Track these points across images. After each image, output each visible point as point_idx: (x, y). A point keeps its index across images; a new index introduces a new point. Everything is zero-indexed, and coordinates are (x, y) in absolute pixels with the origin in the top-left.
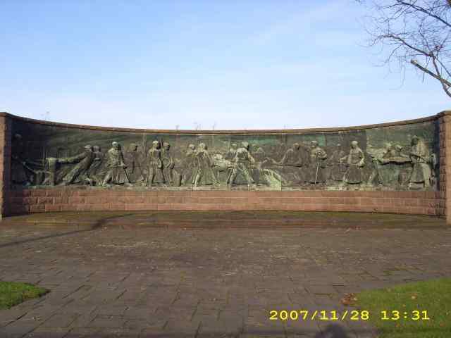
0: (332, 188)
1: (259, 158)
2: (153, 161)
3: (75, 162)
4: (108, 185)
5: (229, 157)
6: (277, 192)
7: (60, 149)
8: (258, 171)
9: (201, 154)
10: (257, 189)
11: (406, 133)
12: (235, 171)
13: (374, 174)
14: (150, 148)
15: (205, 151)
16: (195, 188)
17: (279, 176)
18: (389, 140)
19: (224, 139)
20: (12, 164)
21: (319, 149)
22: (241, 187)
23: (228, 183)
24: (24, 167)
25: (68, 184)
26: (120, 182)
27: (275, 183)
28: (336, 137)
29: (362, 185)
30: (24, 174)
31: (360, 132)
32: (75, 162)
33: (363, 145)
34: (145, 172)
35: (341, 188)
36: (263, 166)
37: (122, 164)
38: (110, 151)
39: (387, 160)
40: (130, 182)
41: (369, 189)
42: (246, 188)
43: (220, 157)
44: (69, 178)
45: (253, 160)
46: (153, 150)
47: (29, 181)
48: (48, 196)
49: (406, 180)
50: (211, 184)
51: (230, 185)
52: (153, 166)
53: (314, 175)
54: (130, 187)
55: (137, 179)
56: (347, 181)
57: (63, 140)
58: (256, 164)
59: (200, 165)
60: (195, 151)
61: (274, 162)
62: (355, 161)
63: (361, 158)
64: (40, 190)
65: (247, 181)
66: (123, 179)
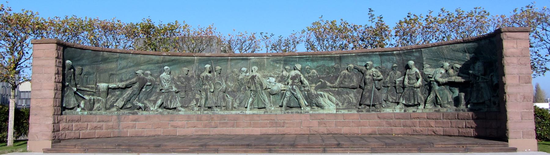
0: (389, 110)
1: (312, 80)
2: (205, 84)
3: (127, 87)
4: (160, 110)
5: (282, 79)
7: (112, 74)
8: (311, 93)
10: (311, 112)
12: (288, 94)
14: (202, 72)
16: (248, 112)
17: (334, 99)
18: (446, 59)
19: (276, 62)
22: (294, 110)
26: (172, 107)
28: (391, 57)
30: (75, 100)
31: (416, 52)
32: (127, 87)
34: (198, 96)
36: (316, 89)
37: (174, 89)
41: (427, 111)
42: (299, 111)
43: (273, 80)
44: (120, 103)
45: (306, 82)
47: (79, 106)
48: (99, 122)
52: (205, 90)
53: (370, 97)
54: (183, 111)
55: (190, 103)
57: (113, 66)
58: (311, 87)
60: (248, 74)
61: (328, 84)
63: (418, 79)
64: (92, 116)
66: (177, 104)
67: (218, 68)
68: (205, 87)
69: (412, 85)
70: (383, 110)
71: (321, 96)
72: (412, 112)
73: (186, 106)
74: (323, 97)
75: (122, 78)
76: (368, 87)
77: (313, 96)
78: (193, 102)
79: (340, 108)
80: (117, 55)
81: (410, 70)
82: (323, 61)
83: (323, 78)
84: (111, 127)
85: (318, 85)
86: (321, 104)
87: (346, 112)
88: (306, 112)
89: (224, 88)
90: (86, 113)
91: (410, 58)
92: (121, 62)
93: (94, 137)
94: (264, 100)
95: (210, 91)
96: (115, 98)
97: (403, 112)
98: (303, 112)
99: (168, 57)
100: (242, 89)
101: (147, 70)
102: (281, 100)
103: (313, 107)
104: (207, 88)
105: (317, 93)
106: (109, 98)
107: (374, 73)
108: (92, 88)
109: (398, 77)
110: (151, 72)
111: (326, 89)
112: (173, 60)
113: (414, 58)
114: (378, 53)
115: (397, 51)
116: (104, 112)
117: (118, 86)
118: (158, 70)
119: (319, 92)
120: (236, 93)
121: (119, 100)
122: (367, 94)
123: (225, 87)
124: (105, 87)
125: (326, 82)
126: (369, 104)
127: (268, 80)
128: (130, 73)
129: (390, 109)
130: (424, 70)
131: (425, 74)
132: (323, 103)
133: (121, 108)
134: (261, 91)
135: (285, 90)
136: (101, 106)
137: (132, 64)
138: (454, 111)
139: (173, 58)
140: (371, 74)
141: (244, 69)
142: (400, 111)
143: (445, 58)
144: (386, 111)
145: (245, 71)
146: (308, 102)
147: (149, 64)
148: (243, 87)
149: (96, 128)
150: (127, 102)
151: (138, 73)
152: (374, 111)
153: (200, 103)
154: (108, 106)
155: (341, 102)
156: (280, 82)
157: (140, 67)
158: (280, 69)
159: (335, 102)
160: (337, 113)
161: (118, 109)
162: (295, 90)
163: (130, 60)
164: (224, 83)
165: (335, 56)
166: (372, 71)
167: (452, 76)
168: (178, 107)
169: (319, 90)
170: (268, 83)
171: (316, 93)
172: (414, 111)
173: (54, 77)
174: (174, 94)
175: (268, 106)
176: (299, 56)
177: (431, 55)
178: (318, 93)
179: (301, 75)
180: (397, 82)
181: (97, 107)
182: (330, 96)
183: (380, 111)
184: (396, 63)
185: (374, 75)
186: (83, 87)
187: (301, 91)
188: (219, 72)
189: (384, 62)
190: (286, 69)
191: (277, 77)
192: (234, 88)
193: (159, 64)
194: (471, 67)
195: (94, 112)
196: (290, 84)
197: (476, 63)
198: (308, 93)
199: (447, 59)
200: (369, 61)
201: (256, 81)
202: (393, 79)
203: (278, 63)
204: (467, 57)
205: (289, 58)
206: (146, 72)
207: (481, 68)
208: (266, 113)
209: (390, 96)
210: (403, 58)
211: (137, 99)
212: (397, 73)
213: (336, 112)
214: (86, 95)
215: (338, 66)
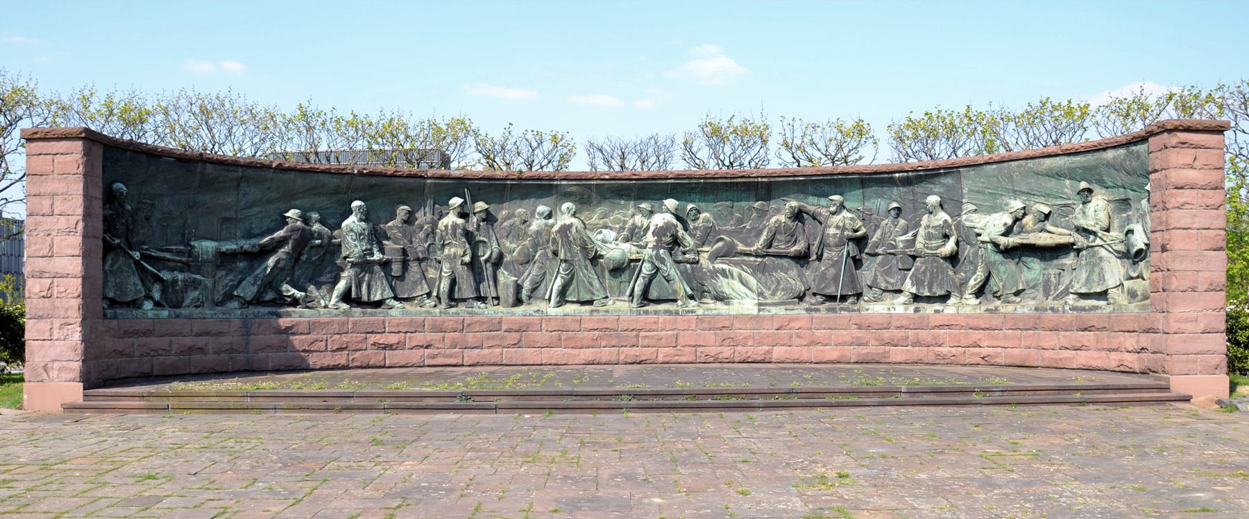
0: (879, 308)
4: (345, 306)
5: (633, 235)
6: (751, 318)
7: (226, 220)
8: (701, 268)
9: (565, 229)
10: (700, 312)
11: (1058, 175)
12: (646, 269)
13: (980, 275)
14: (441, 216)
15: (574, 220)
17: (753, 281)
18: (1016, 193)
20: (104, 260)
23: (632, 294)
24: (137, 263)
25: (246, 304)
27: (744, 302)
29: (952, 300)
30: (138, 282)
33: (951, 204)
34: (432, 273)
35: (899, 306)
36: (714, 257)
38: (346, 223)
39: (1012, 240)
40: (396, 298)
41: (968, 310)
44: (248, 290)
45: (689, 241)
46: (451, 219)
47: (149, 297)
48: (198, 335)
49: (1062, 288)
50: (590, 302)
51: (635, 304)
53: (836, 278)
55: (414, 289)
56: (914, 290)
57: (230, 199)
58: (698, 253)
59: (562, 256)
60: (551, 221)
62: (934, 243)
63: (946, 237)
64: (180, 321)
65: (675, 292)
67: (480, 205)
68: (450, 250)
70: (867, 307)
71: (724, 273)
73: (406, 296)
74: (727, 277)
75: (252, 228)
76: (833, 254)
77: (705, 273)
78: (422, 288)
79: (768, 301)
80: (237, 172)
81: (932, 216)
82: (728, 194)
83: (729, 233)
84: (228, 347)
85: (717, 249)
86: (722, 292)
87: (780, 311)
88: (689, 312)
89: (494, 256)
90: (165, 313)
91: (932, 188)
92: (247, 189)
93: (188, 371)
94: (591, 284)
95: (462, 261)
96: (234, 276)
98: (681, 310)
99: (362, 178)
100: (536, 257)
101: (312, 209)
102: (630, 283)
103: (704, 300)
104: (455, 253)
105: (714, 267)
106: (220, 278)
107: (847, 221)
108: (179, 253)
109: (900, 233)
110: (320, 214)
111: (735, 259)
112: (375, 185)
113: (941, 190)
116: (208, 312)
117: (242, 247)
118: (336, 209)
119: (719, 266)
120: (524, 267)
121: (244, 282)
122: (832, 271)
123: (496, 251)
124: (210, 250)
125: (736, 242)
127: (600, 237)
128: (270, 217)
129: (883, 306)
130: (964, 217)
132: (727, 290)
133: (250, 303)
134: (583, 262)
135: (640, 260)
136: (201, 296)
137: (274, 195)
139: (373, 180)
140: (841, 224)
141: (542, 208)
143: (1015, 191)
144: (873, 309)
145: (547, 213)
146: (692, 289)
147: (315, 195)
148: (539, 252)
149: (191, 350)
150: (265, 286)
151: (288, 217)
152: (845, 310)
153: (439, 289)
154: (218, 297)
155: (769, 289)
156: (627, 240)
157: (293, 203)
158: (628, 210)
159: (755, 288)
160: (761, 313)
161: (243, 304)
162: (663, 261)
163: (268, 186)
164: (495, 245)
165: (758, 182)
167: (1029, 232)
168: (388, 299)
169: (717, 261)
170: (600, 243)
171: (711, 267)
172: (937, 311)
173: (81, 226)
174: (377, 268)
175: (599, 295)
176: (672, 181)
177: (982, 182)
178: (716, 266)
179: (679, 224)
181: (192, 300)
182: (744, 274)
183: (859, 310)
184: (899, 199)
186: (157, 249)
187: (678, 262)
188: (483, 215)
189: (870, 198)
190: (640, 210)
191: (620, 228)
192: (519, 253)
193: (339, 196)
194: (1077, 210)
195: (184, 311)
196: (650, 245)
197: (1090, 202)
198: (692, 268)
201: (571, 239)
203: (622, 195)
204: (1067, 188)
205: (651, 184)
206: (308, 214)
207: (1103, 216)
208: (595, 314)
211: (288, 279)
213: (759, 311)
214: (164, 269)
215: (763, 205)
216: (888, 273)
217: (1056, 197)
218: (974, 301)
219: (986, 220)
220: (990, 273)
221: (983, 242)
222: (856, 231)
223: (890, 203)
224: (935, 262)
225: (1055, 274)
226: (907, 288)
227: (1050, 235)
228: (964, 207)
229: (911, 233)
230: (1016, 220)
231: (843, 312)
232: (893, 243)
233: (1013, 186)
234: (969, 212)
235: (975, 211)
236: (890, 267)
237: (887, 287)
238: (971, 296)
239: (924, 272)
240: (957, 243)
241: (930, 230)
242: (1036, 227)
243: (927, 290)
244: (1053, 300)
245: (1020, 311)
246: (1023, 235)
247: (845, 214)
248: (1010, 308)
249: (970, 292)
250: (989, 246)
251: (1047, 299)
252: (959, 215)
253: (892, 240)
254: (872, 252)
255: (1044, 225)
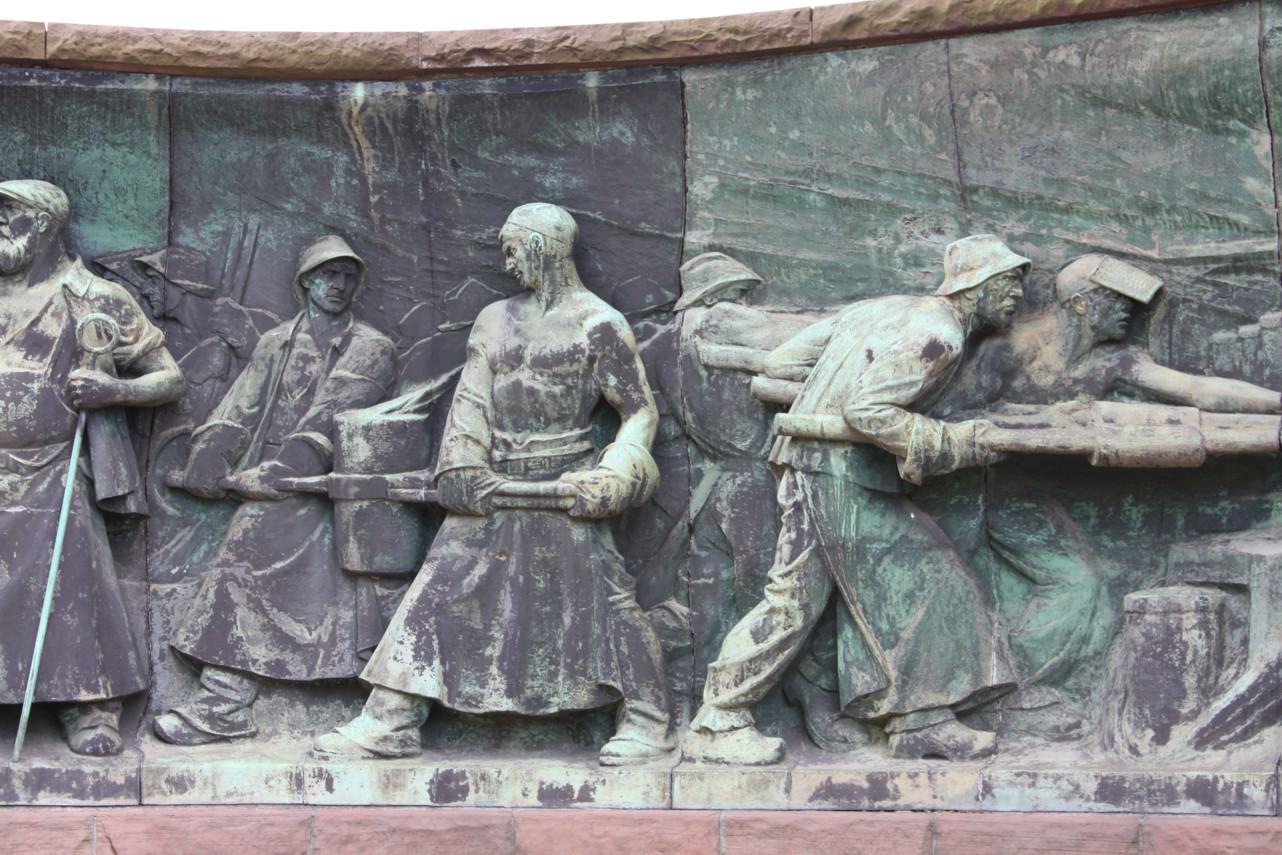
21: (75, 276)
29: (630, 740)
41: (724, 792)
56: (429, 684)
62: (545, 443)
63: (605, 418)
69: (543, 487)
72: (533, 799)
97: (425, 799)
107: (87, 316)
109: (356, 391)
114: (150, 84)
115: (391, 87)
126: (10, 698)
129: (267, 767)
130: (696, 317)
131: (690, 361)
138: (1076, 804)
140: (53, 328)
142: (389, 783)
143: (965, 194)
144: (211, 782)
166: (59, 301)
167: (1041, 397)
172: (554, 796)
177: (798, 147)
180: (360, 441)
183: (135, 787)
184: (354, 222)
185: (89, 341)
189: (207, 207)
199: (994, 193)
200: (26, 175)
202: (301, 410)
204: (1255, 170)
209: (258, 608)
210: (446, 171)
212: (355, 341)
216: (283, 592)
217: (1194, 225)
218: (753, 746)
219: (820, 327)
220: (835, 598)
221: (799, 439)
222: (129, 369)
223: (309, 241)
224: (546, 541)
225: (1202, 610)
226: (395, 669)
227: (1163, 412)
228: (692, 268)
229: (413, 395)
230: (983, 330)
231: (44, 798)
232: (321, 439)
233: (961, 166)
234: (720, 293)
235: (748, 293)
236: (299, 567)
237: (280, 665)
238: (733, 719)
239: (486, 592)
240: (659, 447)
241: (525, 376)
242: (1080, 371)
243: (497, 681)
244: (1202, 740)
245: (1010, 799)
246: (1016, 412)
247: (75, 276)
248: (957, 781)
249: (727, 696)
250: (838, 463)
251: (1162, 738)
252: (667, 310)
253: (315, 424)
254: (208, 485)
255: (1127, 363)
